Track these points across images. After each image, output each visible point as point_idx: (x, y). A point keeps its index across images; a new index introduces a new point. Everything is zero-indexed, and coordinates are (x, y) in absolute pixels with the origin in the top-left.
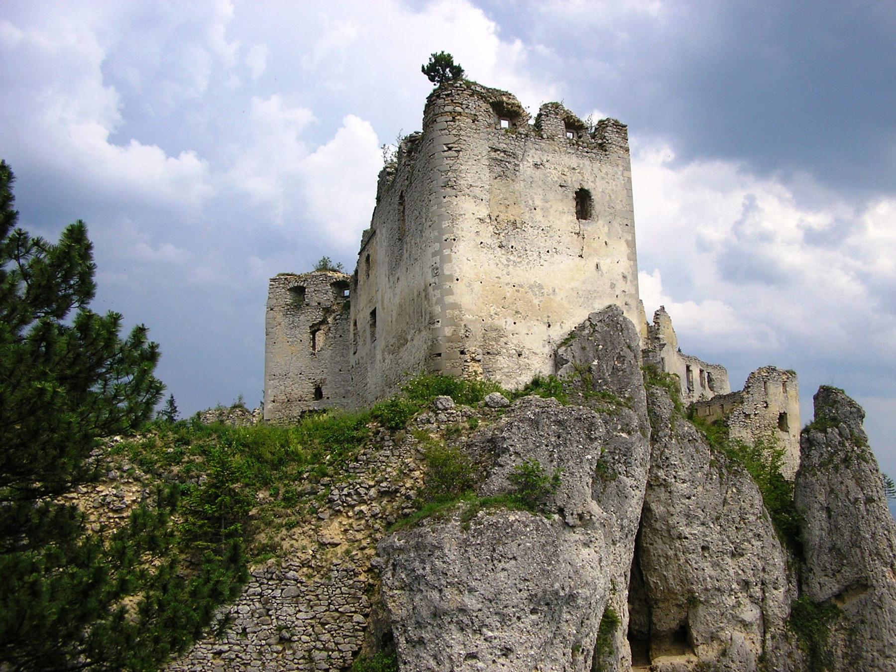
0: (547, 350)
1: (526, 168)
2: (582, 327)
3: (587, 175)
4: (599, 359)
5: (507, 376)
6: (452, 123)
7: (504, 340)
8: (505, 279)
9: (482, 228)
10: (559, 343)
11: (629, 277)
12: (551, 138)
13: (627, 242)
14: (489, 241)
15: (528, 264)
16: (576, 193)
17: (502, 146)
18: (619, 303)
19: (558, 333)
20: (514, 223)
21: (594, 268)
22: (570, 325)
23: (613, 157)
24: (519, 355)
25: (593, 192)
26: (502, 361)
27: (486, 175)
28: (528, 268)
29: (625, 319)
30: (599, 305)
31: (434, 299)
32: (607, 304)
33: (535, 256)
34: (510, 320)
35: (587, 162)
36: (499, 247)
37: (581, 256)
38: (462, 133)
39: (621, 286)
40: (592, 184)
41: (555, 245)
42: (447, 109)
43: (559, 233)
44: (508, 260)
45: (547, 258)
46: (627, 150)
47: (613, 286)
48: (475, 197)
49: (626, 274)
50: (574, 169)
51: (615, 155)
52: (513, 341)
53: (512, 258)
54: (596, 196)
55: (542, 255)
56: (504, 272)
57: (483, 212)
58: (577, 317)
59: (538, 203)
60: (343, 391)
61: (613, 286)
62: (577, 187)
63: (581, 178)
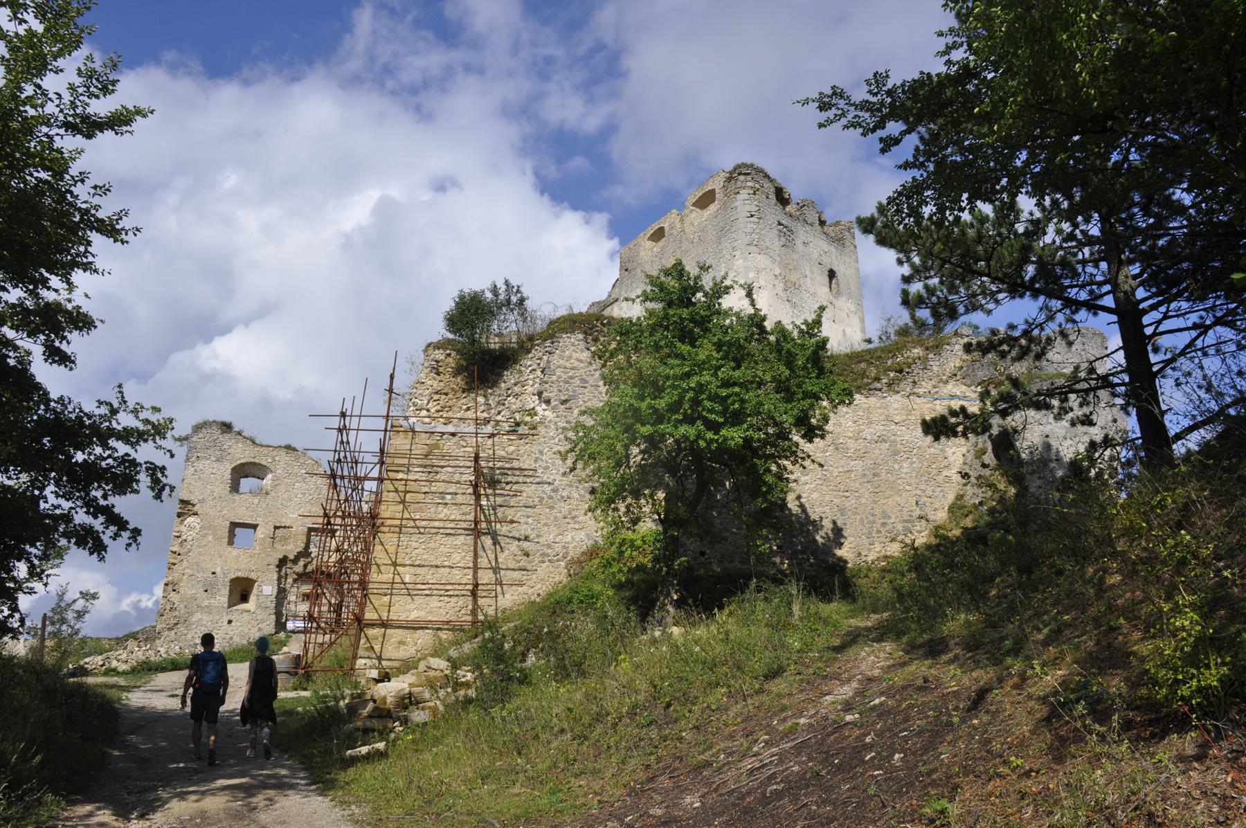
3: (834, 260)
9: (776, 282)
23: (847, 250)
42: (749, 184)
59: (808, 273)
62: (829, 267)
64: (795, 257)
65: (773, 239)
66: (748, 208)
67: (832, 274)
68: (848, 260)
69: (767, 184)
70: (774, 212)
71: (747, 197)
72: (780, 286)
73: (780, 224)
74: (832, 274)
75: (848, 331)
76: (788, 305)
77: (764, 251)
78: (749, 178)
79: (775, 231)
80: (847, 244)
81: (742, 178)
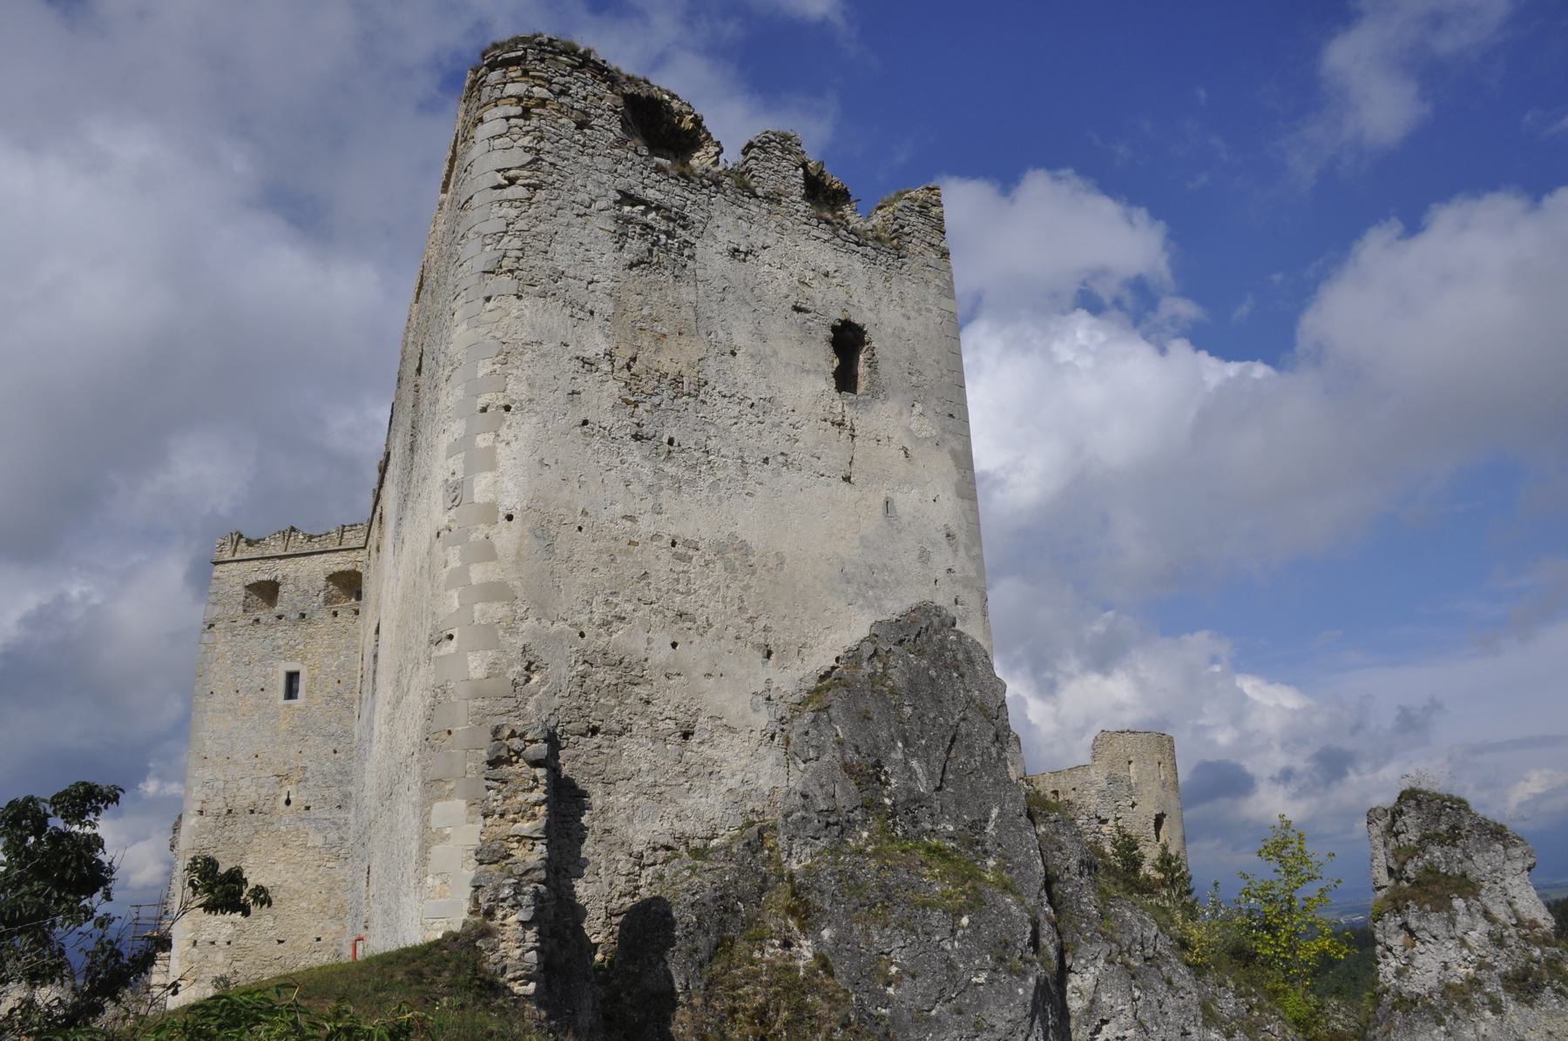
0: (763, 719)
1: (711, 256)
2: (853, 656)
4: (906, 744)
5: (651, 797)
6: (521, 122)
7: (643, 691)
8: (646, 525)
9: (587, 383)
10: (796, 698)
11: (962, 537)
12: (773, 198)
13: (953, 453)
14: (608, 420)
15: (714, 486)
16: (834, 329)
17: (651, 194)
18: (942, 599)
19: (793, 677)
20: (677, 381)
21: (880, 511)
22: (822, 659)
23: (913, 264)
24: (686, 735)
25: (872, 334)
26: (637, 752)
27: (606, 260)
28: (715, 500)
29: (960, 634)
30: (895, 606)
31: (444, 574)
32: (911, 601)
33: (732, 470)
34: (662, 639)
35: (858, 266)
36: (636, 437)
37: (847, 479)
38: (546, 146)
39: (942, 558)
40: (870, 315)
41: (784, 446)
42: (511, 89)
43: (794, 418)
44: (657, 472)
45: (766, 473)
46: (945, 254)
47: (924, 557)
48: (571, 303)
49: (954, 529)
50: (827, 275)
51: (920, 259)
52: (669, 701)
53: (670, 469)
54: (879, 340)
55: (751, 469)
56: (648, 504)
57: (596, 345)
58: (849, 628)
59: (741, 339)
60: (337, 796)
61: (924, 557)
62: (836, 315)
63: (845, 297)
64: (686, 293)
65: (592, 250)
66: (499, 159)
67: (847, 340)
68: (910, 289)
69: (582, 88)
70: (607, 167)
71: (500, 126)
72: (602, 395)
73: (627, 198)
74: (847, 340)
75: (906, 501)
76: (636, 453)
77: (550, 286)
78: (515, 72)
79: (602, 224)
80: (915, 246)
81: (495, 76)
